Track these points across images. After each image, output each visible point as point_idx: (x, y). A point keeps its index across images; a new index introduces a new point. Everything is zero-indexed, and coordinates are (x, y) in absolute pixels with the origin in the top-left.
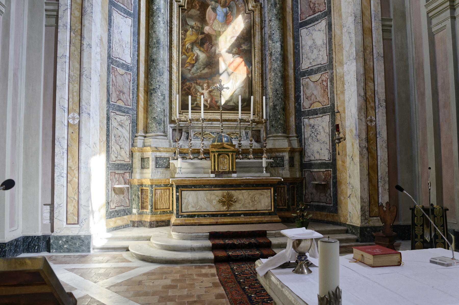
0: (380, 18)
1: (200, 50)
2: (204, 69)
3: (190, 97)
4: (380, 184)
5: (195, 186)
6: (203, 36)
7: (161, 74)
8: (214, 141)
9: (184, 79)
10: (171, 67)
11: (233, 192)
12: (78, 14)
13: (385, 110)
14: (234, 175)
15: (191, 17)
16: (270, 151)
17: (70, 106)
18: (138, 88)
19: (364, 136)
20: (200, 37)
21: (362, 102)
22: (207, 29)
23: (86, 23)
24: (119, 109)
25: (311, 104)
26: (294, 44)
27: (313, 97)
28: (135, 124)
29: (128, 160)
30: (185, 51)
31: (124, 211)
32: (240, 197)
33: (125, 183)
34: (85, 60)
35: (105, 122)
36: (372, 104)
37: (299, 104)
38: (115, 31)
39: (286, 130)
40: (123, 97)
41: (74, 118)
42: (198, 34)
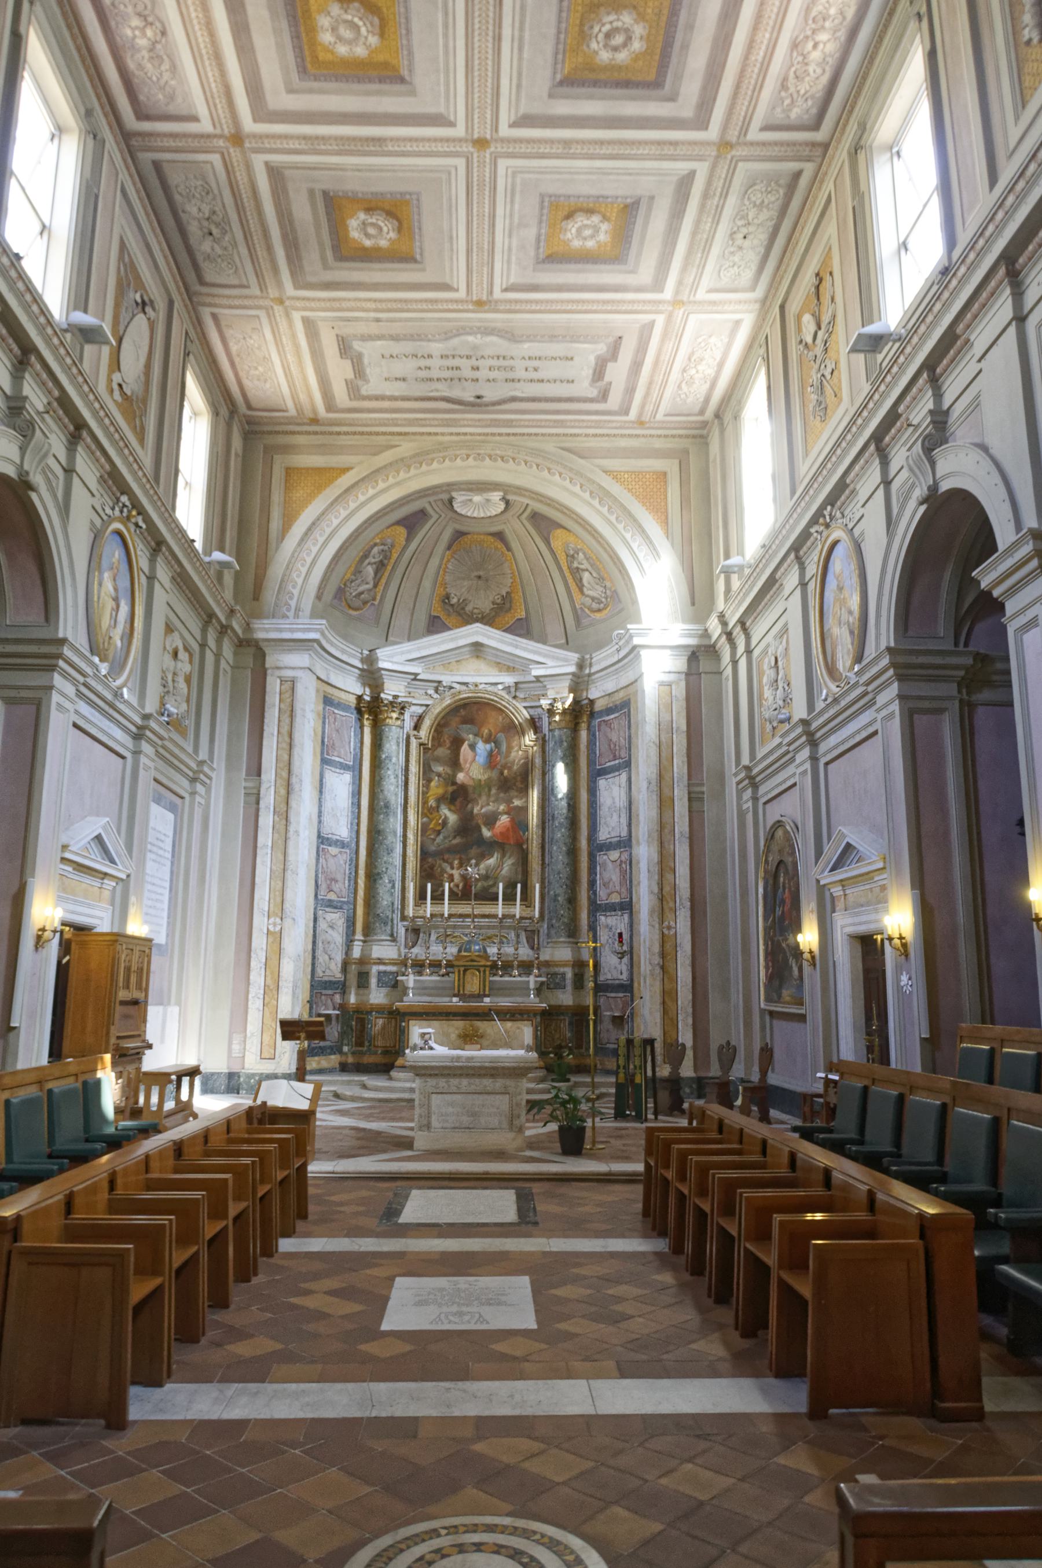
0: (686, 782)
1: (450, 810)
2: (455, 837)
3: (429, 885)
4: (680, 1018)
5: (427, 1014)
6: (455, 787)
7: (390, 851)
8: (460, 951)
9: (424, 854)
10: (405, 836)
11: (478, 1024)
12: (283, 792)
13: (688, 914)
14: (487, 1000)
15: (437, 760)
16: (547, 964)
17: (272, 909)
18: (356, 872)
19: (657, 949)
20: (451, 789)
21: (656, 902)
22: (461, 777)
23: (293, 803)
24: (330, 904)
25: (609, 895)
26: (589, 800)
27: (611, 884)
28: (351, 923)
29: (339, 976)
30: (427, 812)
31: (331, 1048)
32: (489, 1031)
33: (334, 1009)
34: (291, 850)
35: (312, 925)
36: (671, 904)
37: (595, 893)
38: (327, 796)
39: (573, 932)
40: (336, 887)
41: (275, 925)
42: (447, 785)
